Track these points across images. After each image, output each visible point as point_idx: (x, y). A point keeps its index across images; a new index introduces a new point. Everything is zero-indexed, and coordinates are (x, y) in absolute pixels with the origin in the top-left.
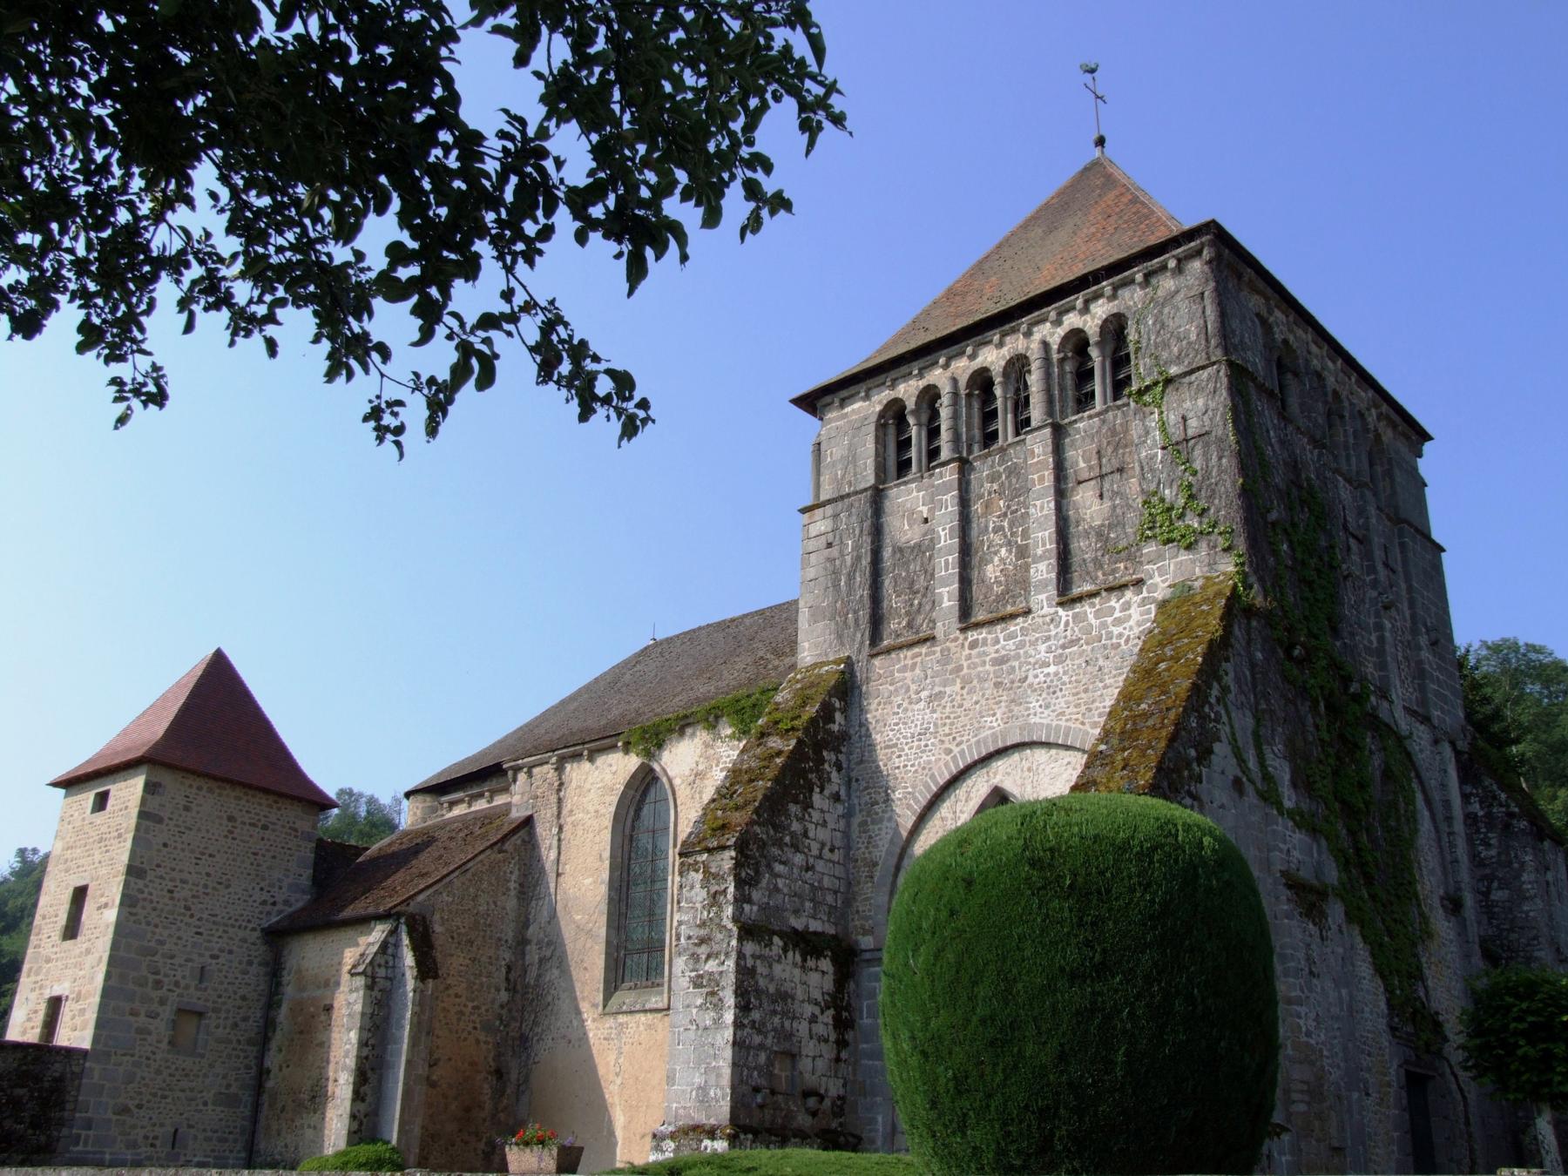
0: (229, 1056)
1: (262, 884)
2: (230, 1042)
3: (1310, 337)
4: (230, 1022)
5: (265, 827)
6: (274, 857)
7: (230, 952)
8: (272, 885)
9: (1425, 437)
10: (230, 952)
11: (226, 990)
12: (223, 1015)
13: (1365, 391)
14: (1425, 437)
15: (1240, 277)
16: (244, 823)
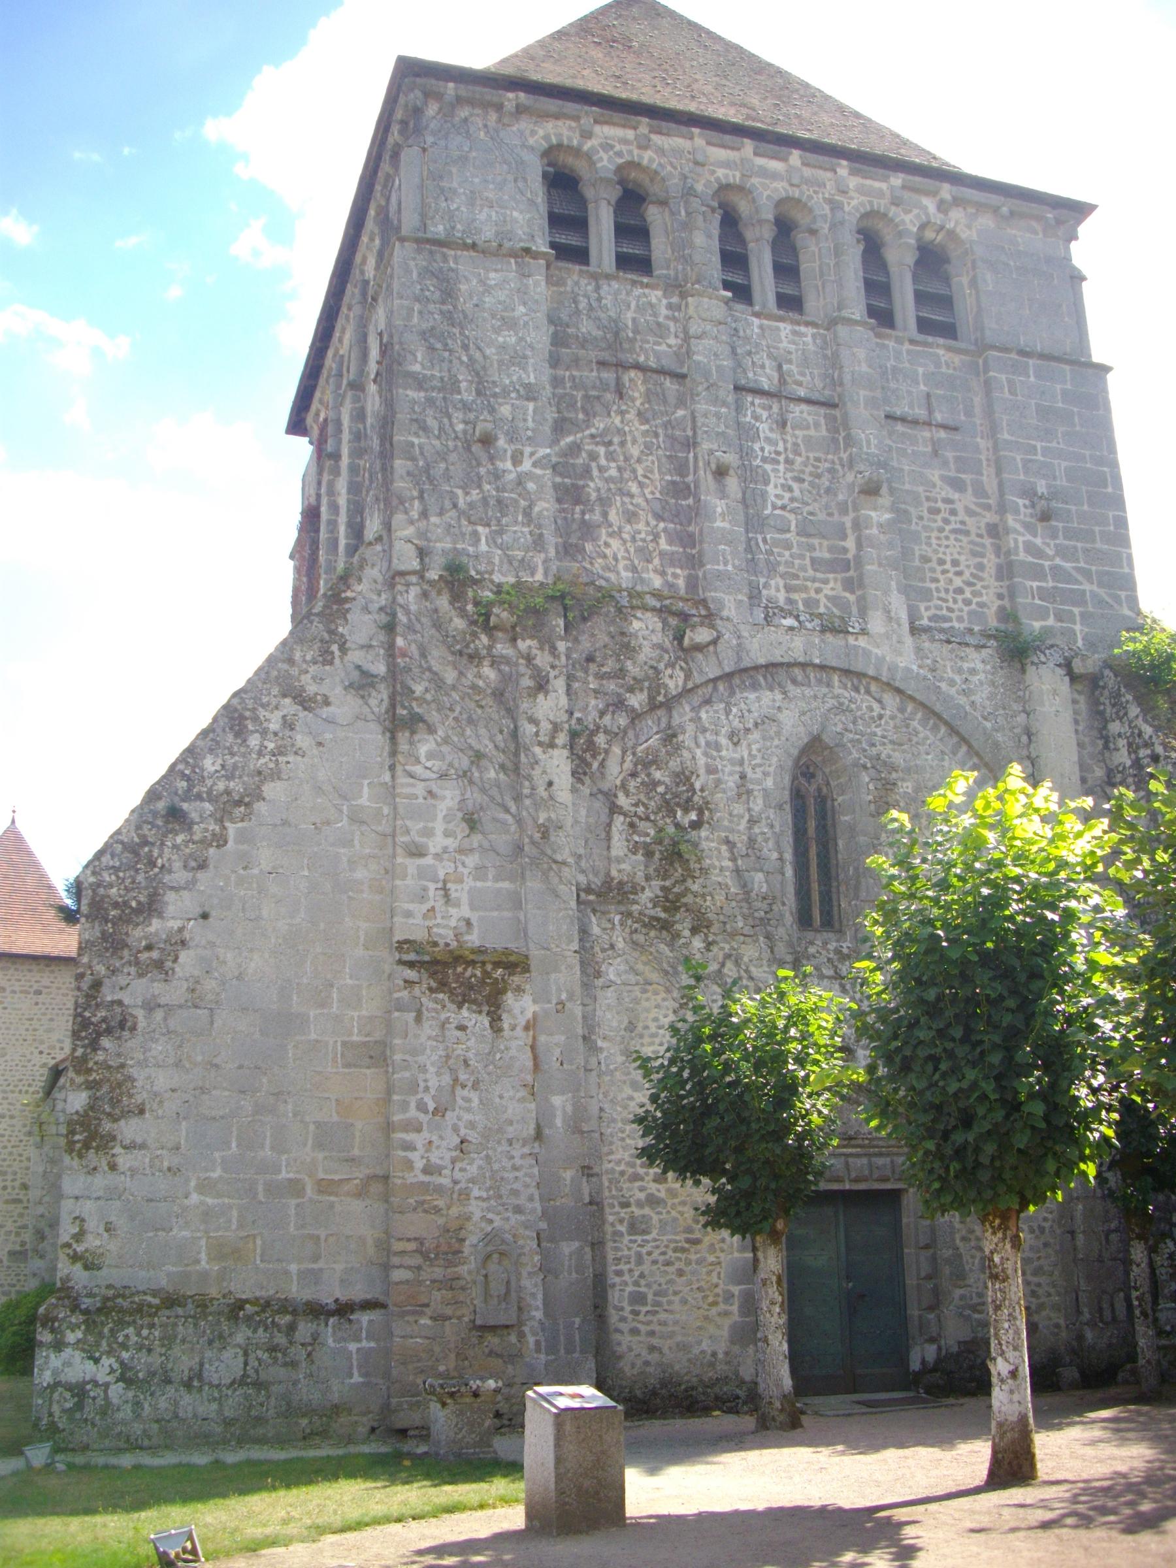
0: (21, 1215)
1: (41, 1048)
2: (19, 1201)
3: (699, 142)
4: (17, 1184)
5: (38, 993)
6: (51, 1020)
7: (12, 1117)
8: (53, 1047)
9: (1079, 210)
10: (12, 1117)
11: (11, 1154)
12: (10, 1177)
13: (885, 179)
14: (1079, 210)
15: (499, 107)
16: (14, 992)
